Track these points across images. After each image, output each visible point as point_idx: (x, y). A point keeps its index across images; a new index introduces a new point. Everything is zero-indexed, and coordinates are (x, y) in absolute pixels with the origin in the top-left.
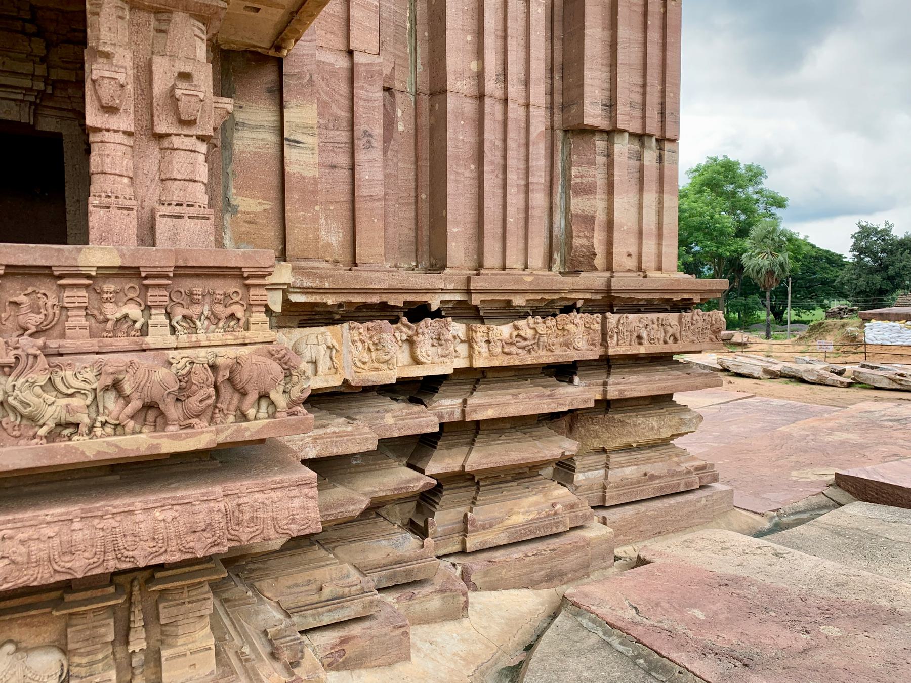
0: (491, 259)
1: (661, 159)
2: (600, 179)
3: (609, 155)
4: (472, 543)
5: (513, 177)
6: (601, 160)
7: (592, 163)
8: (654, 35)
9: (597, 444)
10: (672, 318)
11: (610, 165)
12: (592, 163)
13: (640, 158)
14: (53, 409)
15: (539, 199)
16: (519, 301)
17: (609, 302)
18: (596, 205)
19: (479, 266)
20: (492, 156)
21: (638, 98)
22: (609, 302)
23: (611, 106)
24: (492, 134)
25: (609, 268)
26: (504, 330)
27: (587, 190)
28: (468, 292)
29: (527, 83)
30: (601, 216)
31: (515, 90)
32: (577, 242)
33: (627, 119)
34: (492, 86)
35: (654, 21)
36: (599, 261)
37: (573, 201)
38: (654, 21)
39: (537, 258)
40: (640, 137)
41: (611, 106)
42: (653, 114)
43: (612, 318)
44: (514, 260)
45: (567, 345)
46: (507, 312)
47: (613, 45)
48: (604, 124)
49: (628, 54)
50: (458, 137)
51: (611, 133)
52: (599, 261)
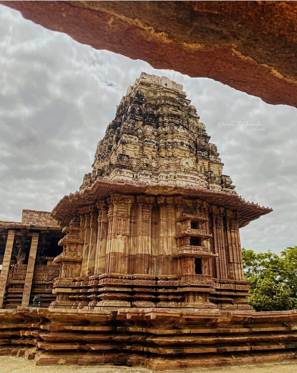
0: (222, 278)
1: (241, 266)
2: (233, 268)
3: (234, 265)
4: (222, 308)
5: (223, 269)
6: (233, 266)
7: (232, 267)
8: (238, 251)
9: (236, 302)
10: (244, 286)
11: (234, 267)
12: (232, 267)
13: (238, 266)
14: (204, 283)
15: (226, 271)
16: (225, 282)
17: (235, 283)
18: (233, 271)
19: (221, 278)
20: (221, 266)
21: (236, 259)
22: (235, 283)
23: (233, 260)
24: (221, 264)
25: (235, 279)
26: (224, 285)
27: (232, 270)
28: (220, 281)
29: (224, 259)
30: (234, 273)
31: (223, 260)
32: (231, 276)
33: (235, 261)
34: (220, 259)
35: (237, 250)
36: (234, 278)
37: (230, 271)
38: (237, 250)
39: (227, 277)
40: (238, 263)
41: (233, 260)
42: (239, 261)
43: (236, 285)
44: (224, 278)
45: (231, 287)
46: (224, 283)
47: (233, 253)
48: (233, 262)
49: (235, 253)
50: (217, 265)
51: (234, 263)
52: (234, 278)
